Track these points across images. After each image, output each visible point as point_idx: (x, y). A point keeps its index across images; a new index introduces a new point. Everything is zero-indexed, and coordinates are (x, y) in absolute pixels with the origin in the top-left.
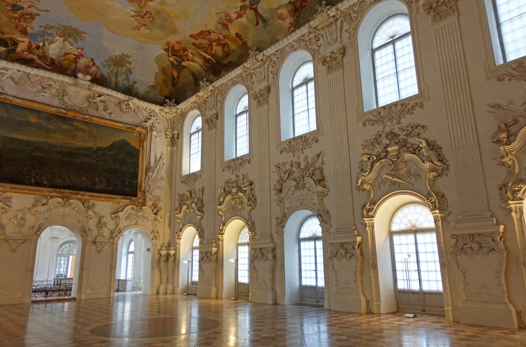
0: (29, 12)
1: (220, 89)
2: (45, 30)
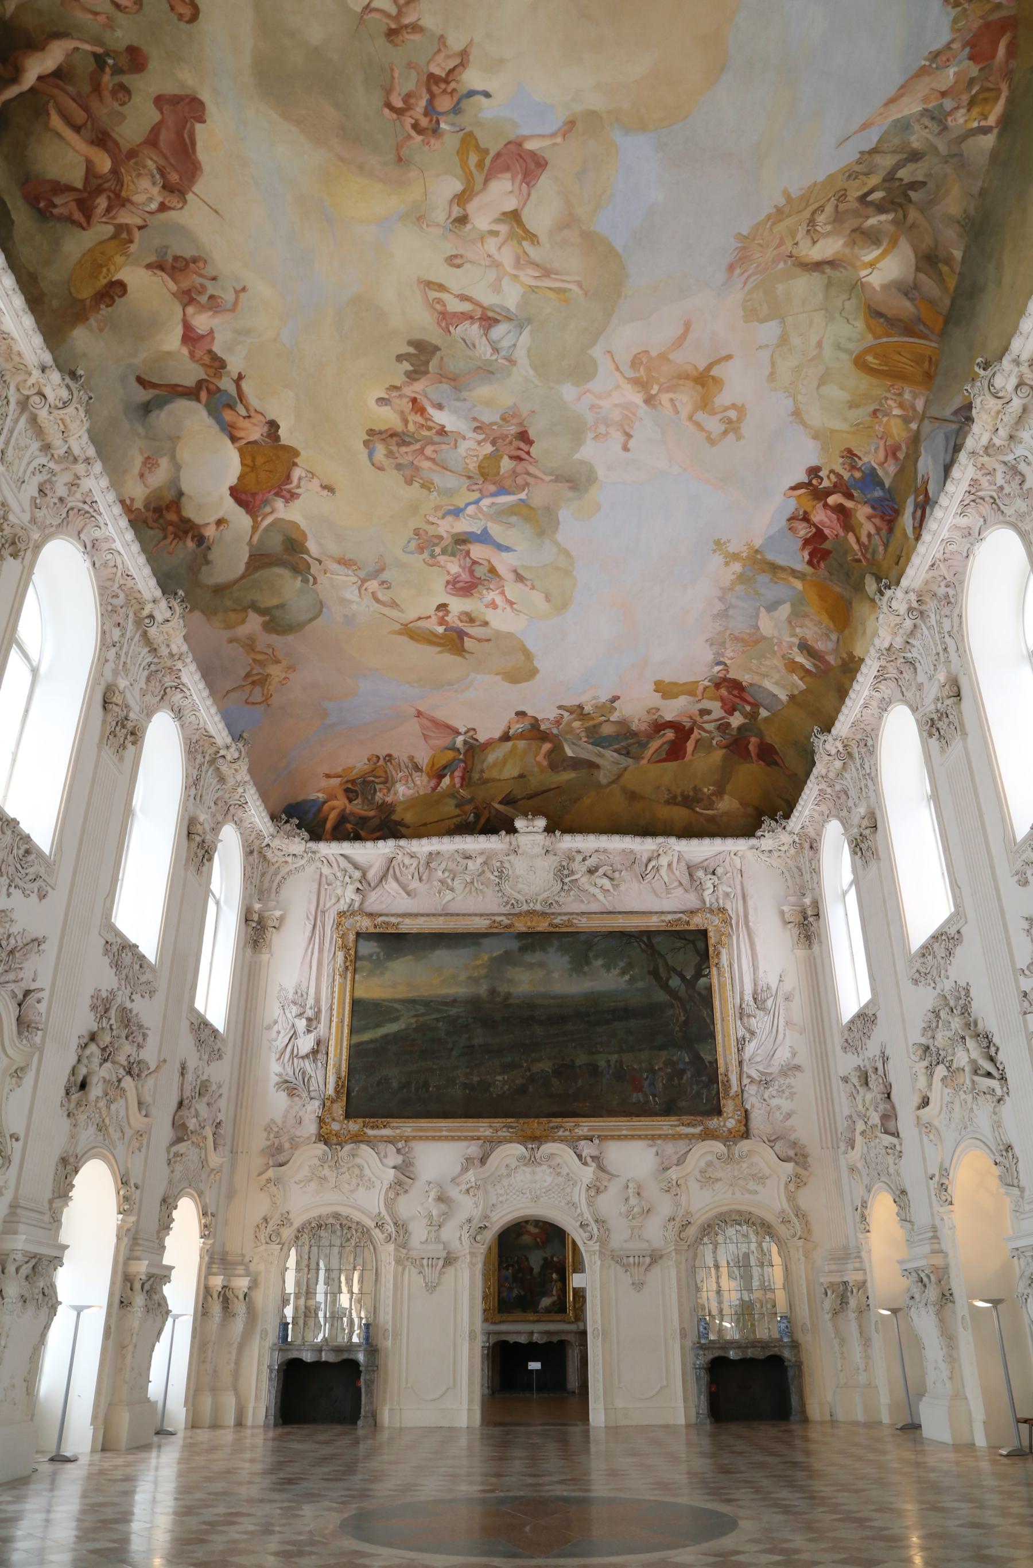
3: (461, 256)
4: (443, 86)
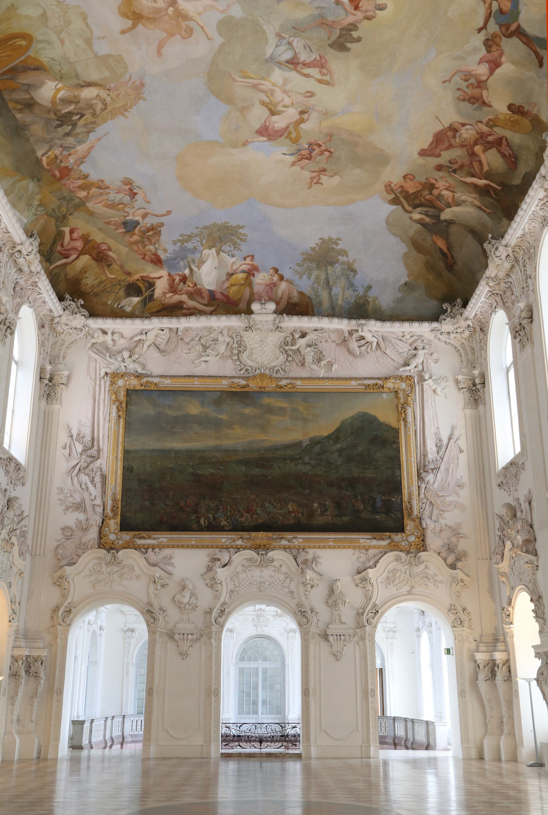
0: (149, 225)
1: (524, 247)
2: (183, 246)
3: (306, 97)
4: (304, 157)
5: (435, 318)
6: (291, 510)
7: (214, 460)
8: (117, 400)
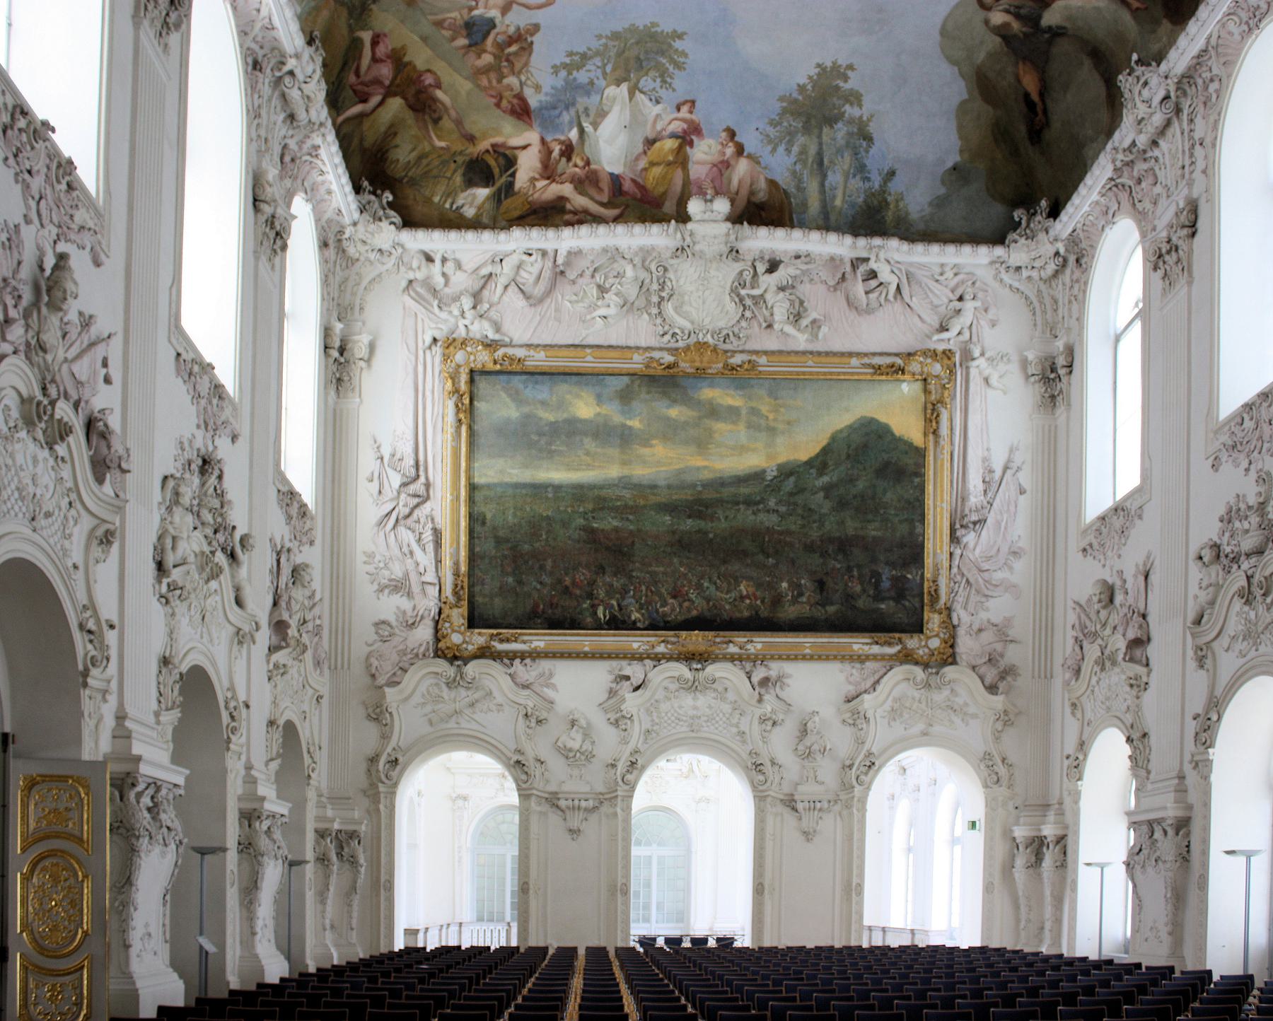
5: (998, 239)
6: (745, 593)
7: (619, 503)
8: (456, 391)
